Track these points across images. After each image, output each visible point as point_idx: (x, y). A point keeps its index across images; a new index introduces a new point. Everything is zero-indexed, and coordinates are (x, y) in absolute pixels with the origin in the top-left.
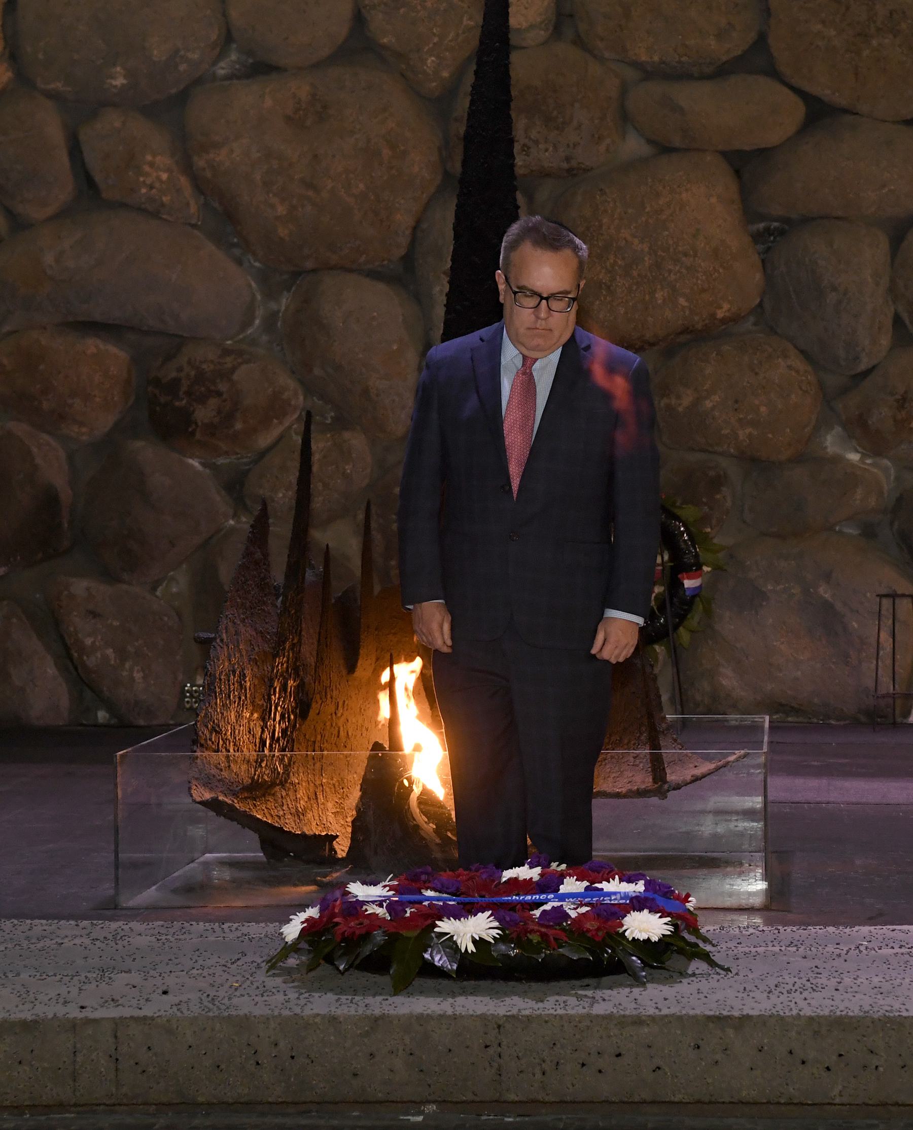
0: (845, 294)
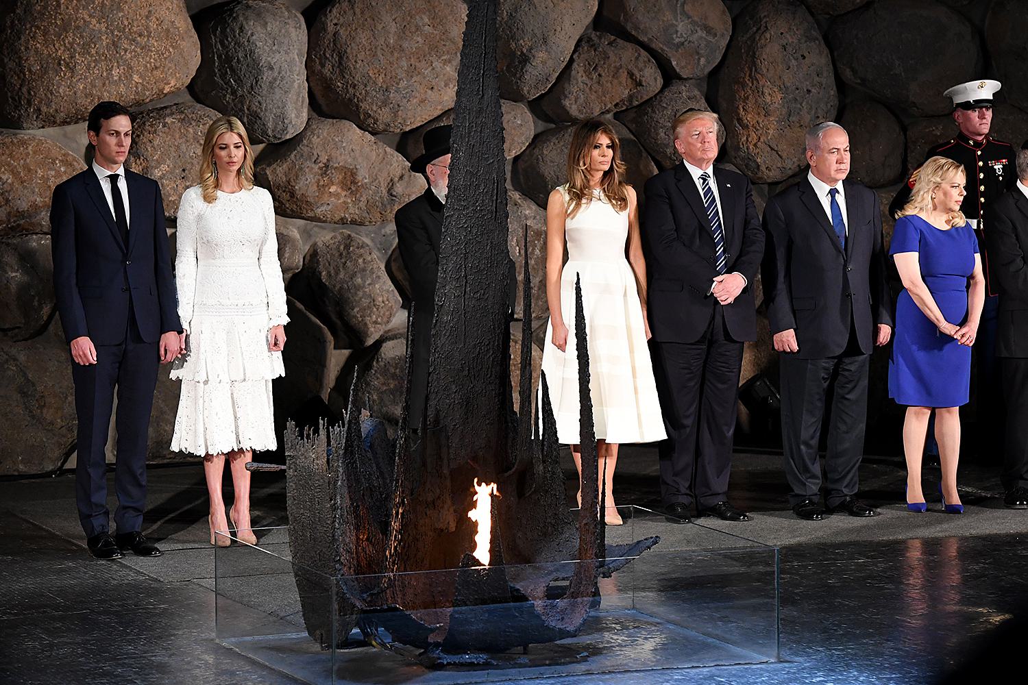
0: (279, 73)
